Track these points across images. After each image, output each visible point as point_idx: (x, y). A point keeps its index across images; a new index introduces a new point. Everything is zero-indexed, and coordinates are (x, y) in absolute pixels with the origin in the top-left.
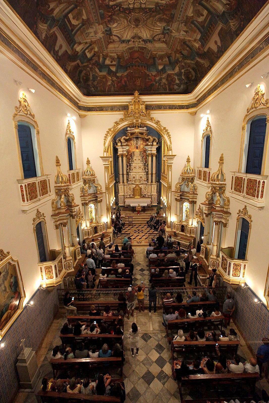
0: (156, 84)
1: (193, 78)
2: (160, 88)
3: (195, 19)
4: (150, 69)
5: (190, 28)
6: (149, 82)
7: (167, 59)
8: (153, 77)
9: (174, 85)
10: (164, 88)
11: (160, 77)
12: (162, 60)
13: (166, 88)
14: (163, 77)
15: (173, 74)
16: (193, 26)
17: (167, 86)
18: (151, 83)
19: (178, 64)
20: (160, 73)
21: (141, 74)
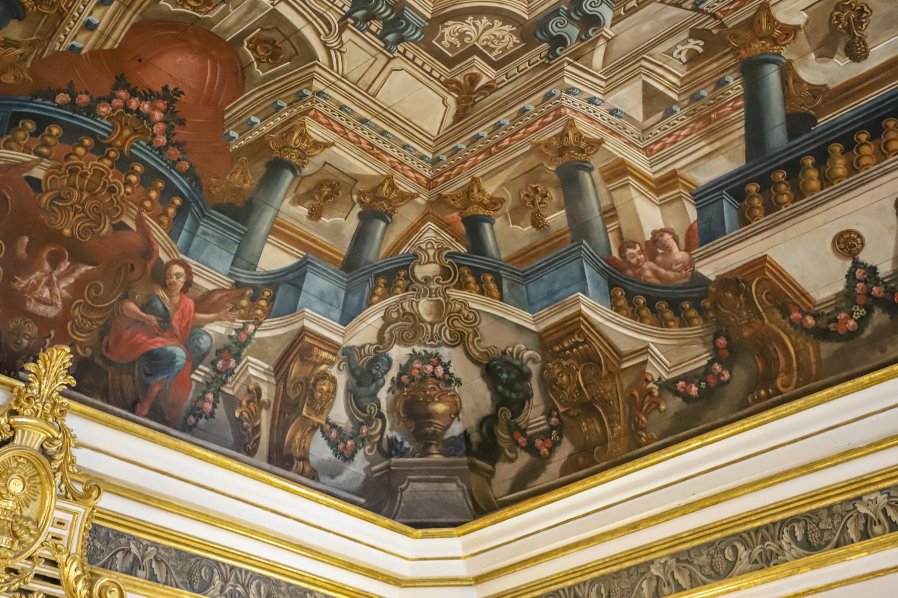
0: (195, 367)
1: (456, 429)
2: (208, 406)
3: (786, 54)
4: (192, 234)
5: (704, 93)
6: (140, 323)
7: (351, 225)
8: (191, 303)
9: (314, 429)
10: (240, 420)
11: (244, 329)
12: (315, 214)
13: (257, 429)
14: (258, 335)
15: (333, 347)
16: (735, 86)
17: (265, 419)
18: (159, 343)
19: (389, 293)
20: (254, 299)
21: (106, 229)
